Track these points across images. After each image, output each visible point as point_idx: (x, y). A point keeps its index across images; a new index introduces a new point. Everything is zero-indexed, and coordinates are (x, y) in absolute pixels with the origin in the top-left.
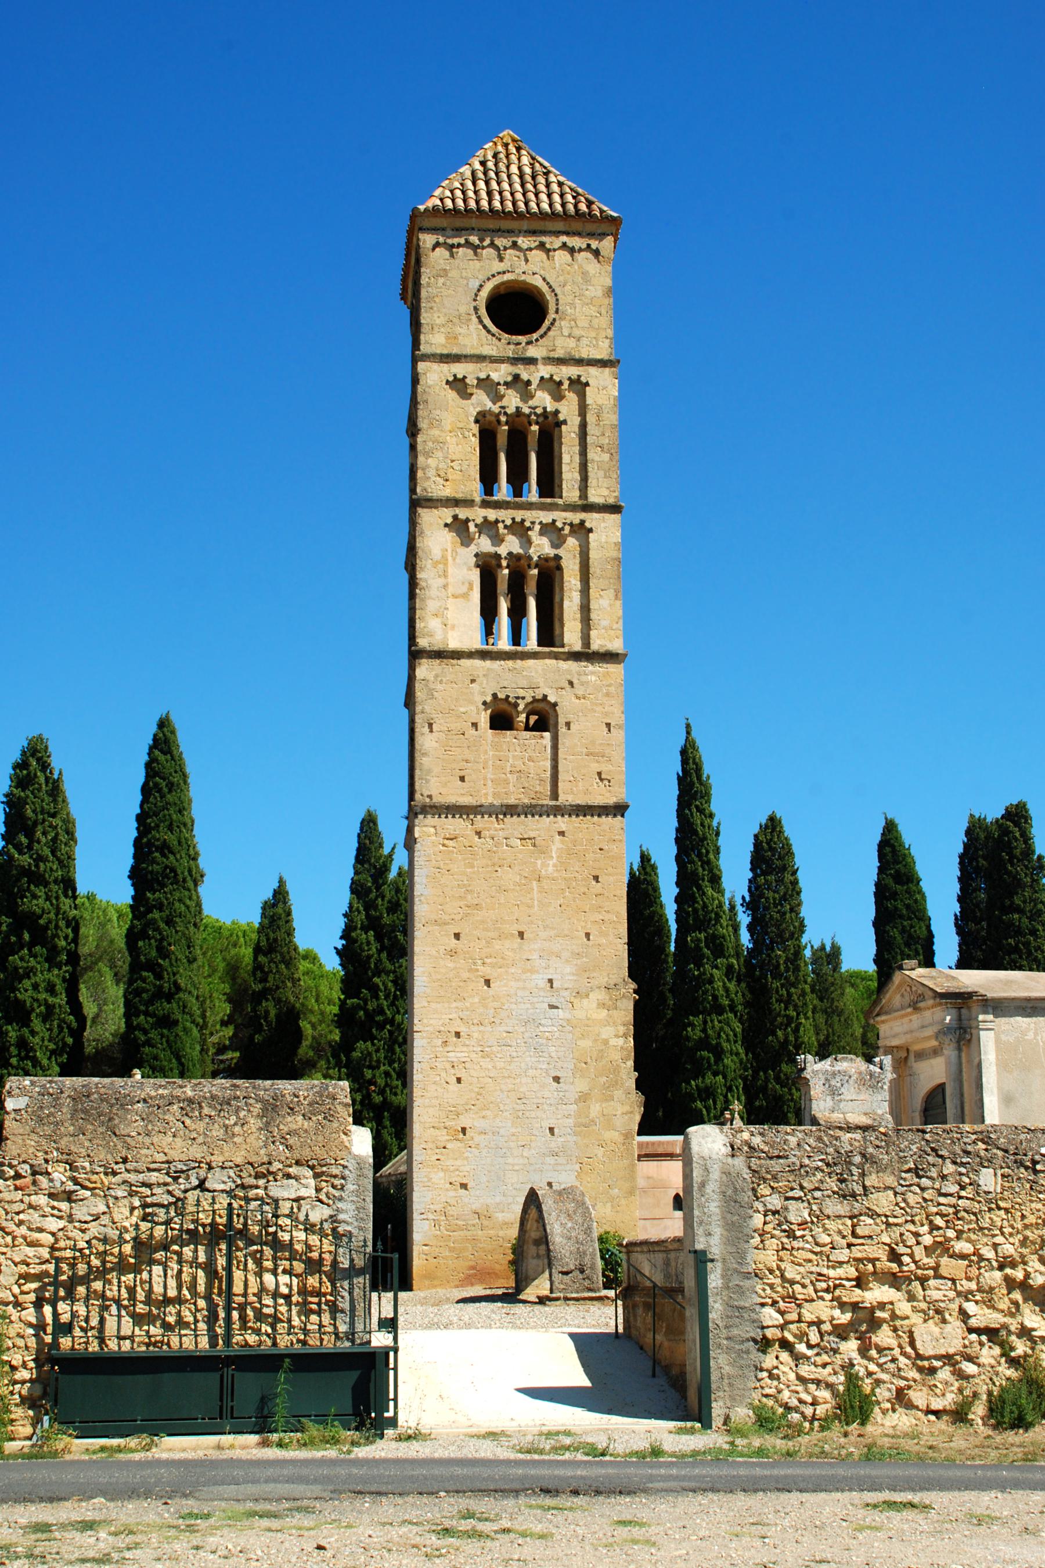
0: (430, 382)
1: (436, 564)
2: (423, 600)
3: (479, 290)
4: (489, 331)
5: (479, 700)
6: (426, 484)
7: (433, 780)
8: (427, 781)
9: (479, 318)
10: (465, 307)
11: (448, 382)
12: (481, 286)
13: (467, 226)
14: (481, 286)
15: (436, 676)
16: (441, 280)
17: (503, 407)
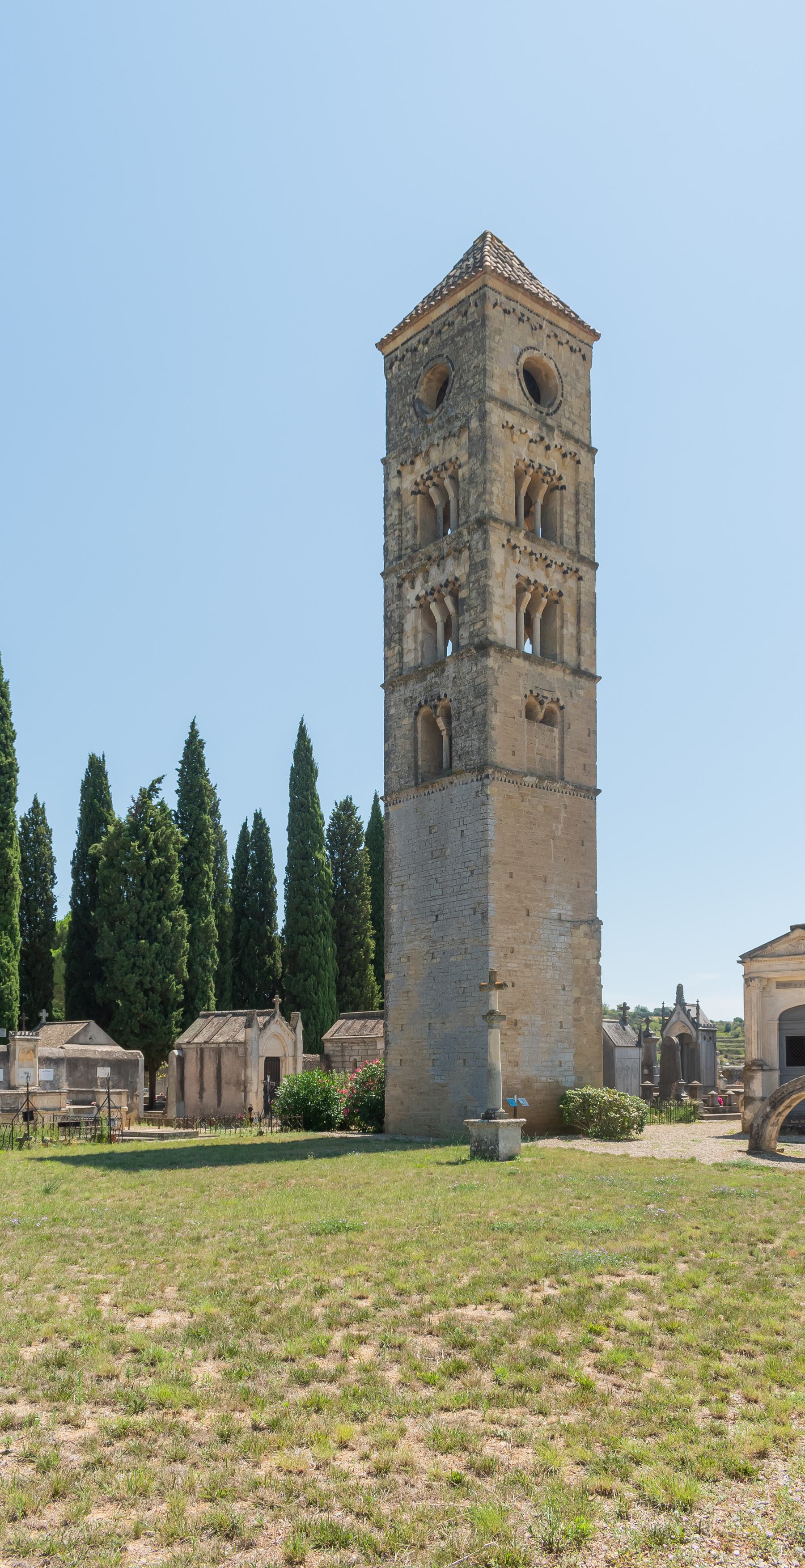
0: (493, 422)
1: (498, 576)
2: (491, 603)
3: (519, 357)
4: (525, 394)
5: (523, 692)
6: (492, 507)
7: (498, 750)
8: (495, 750)
9: (519, 379)
10: (512, 368)
11: (503, 427)
12: (521, 354)
13: (515, 299)
14: (521, 354)
15: (499, 668)
16: (497, 338)
17: (531, 461)
